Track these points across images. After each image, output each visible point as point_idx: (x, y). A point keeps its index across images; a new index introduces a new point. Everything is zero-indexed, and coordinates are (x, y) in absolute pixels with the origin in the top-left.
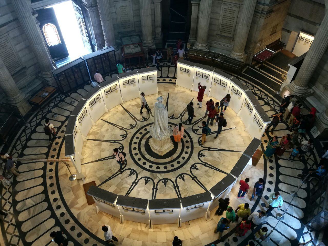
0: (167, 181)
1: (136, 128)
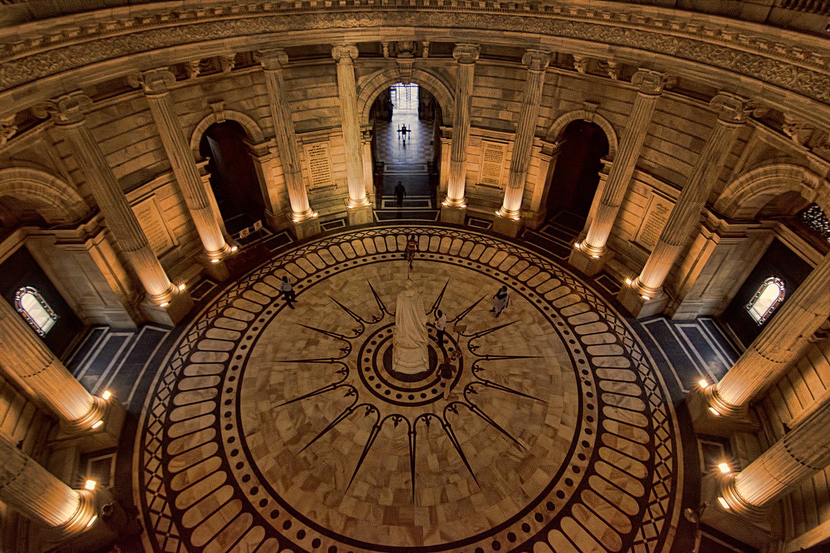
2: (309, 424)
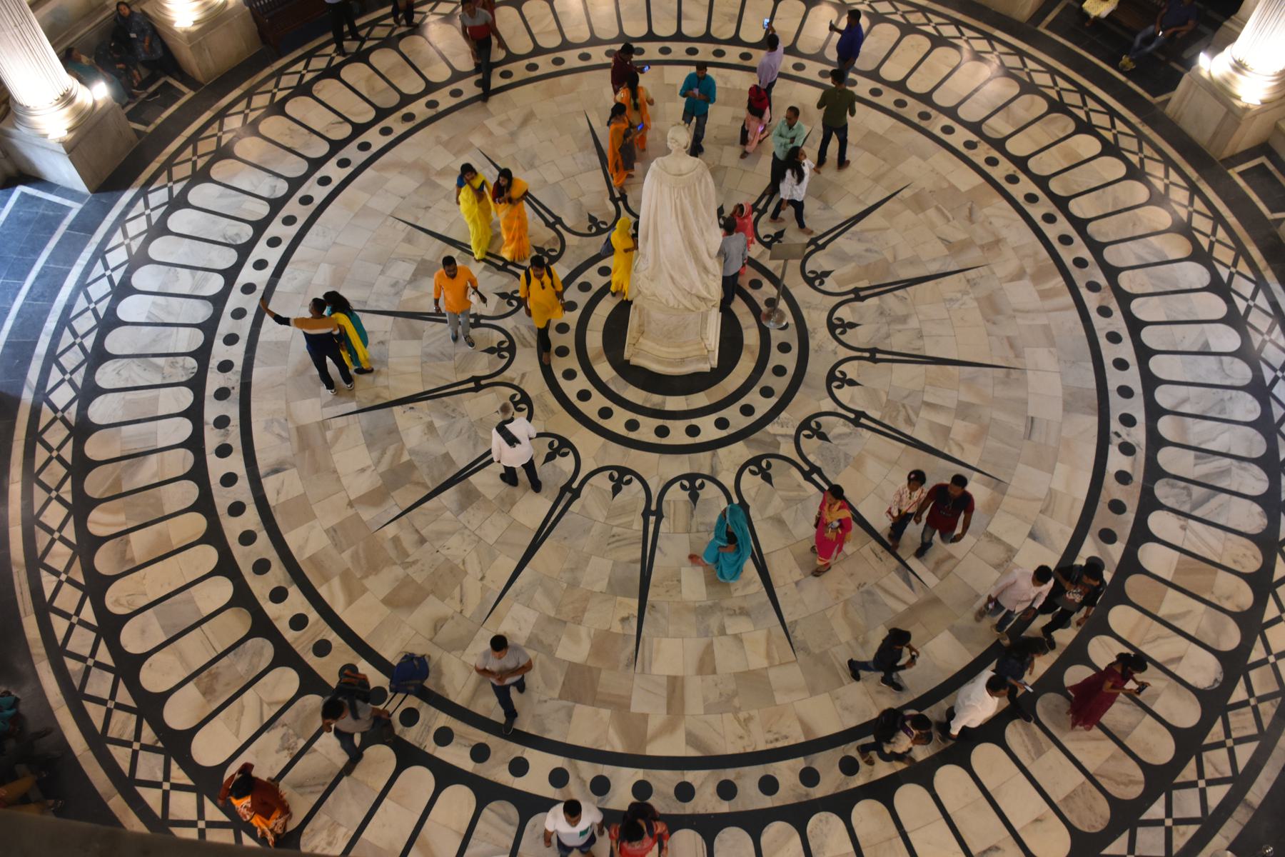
1: (525, 346)
2: (410, 466)
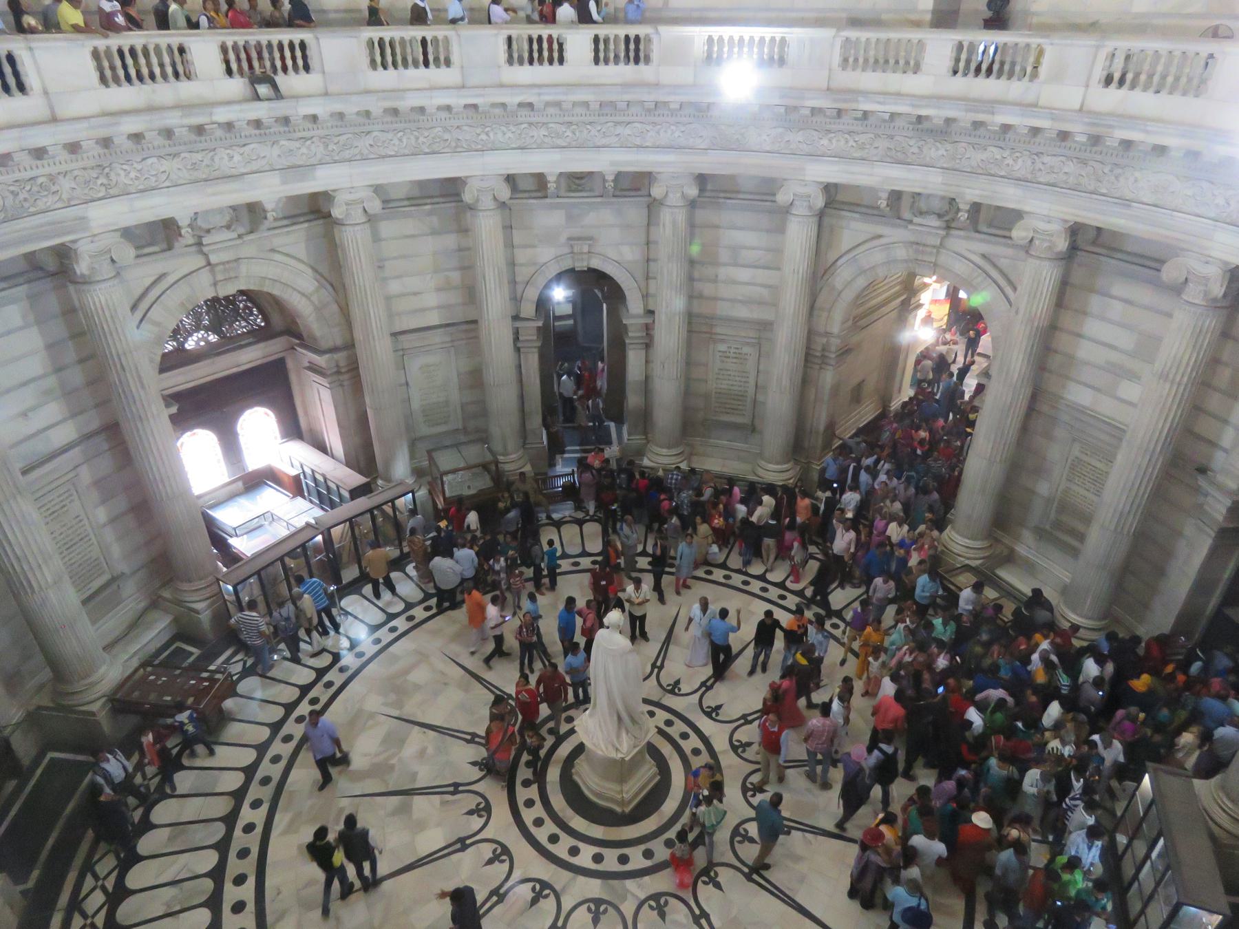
0: (666, 903)
